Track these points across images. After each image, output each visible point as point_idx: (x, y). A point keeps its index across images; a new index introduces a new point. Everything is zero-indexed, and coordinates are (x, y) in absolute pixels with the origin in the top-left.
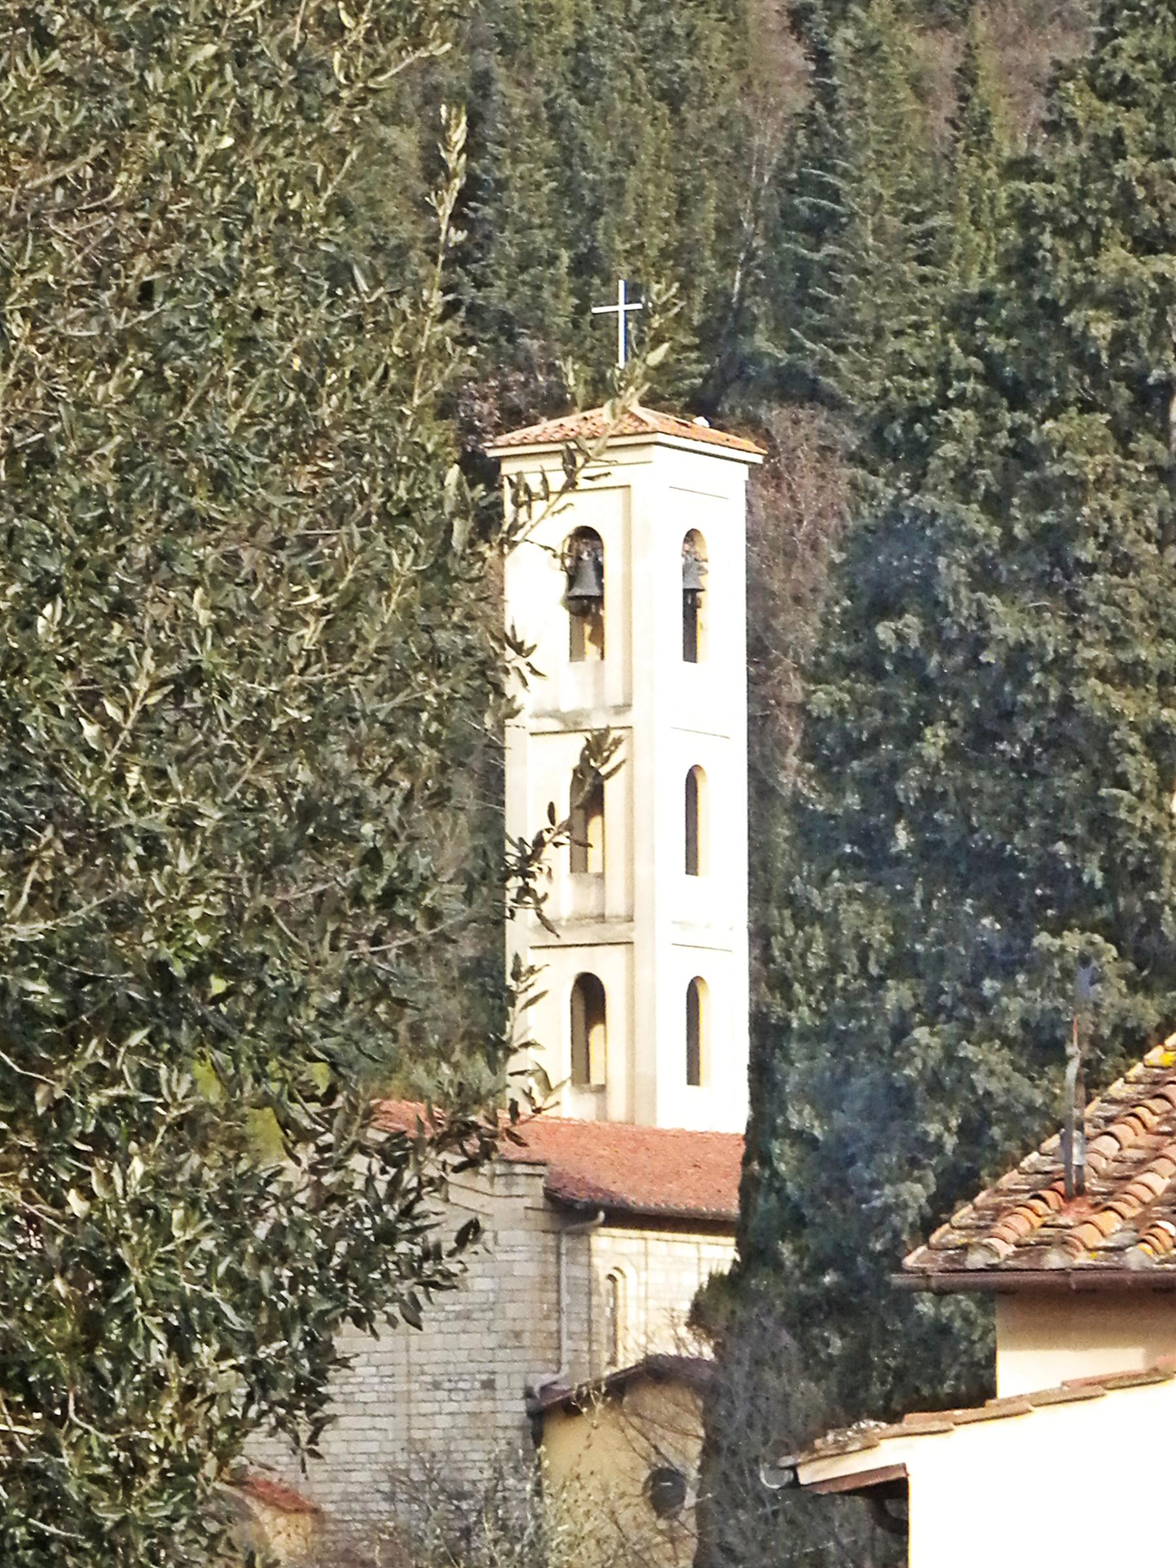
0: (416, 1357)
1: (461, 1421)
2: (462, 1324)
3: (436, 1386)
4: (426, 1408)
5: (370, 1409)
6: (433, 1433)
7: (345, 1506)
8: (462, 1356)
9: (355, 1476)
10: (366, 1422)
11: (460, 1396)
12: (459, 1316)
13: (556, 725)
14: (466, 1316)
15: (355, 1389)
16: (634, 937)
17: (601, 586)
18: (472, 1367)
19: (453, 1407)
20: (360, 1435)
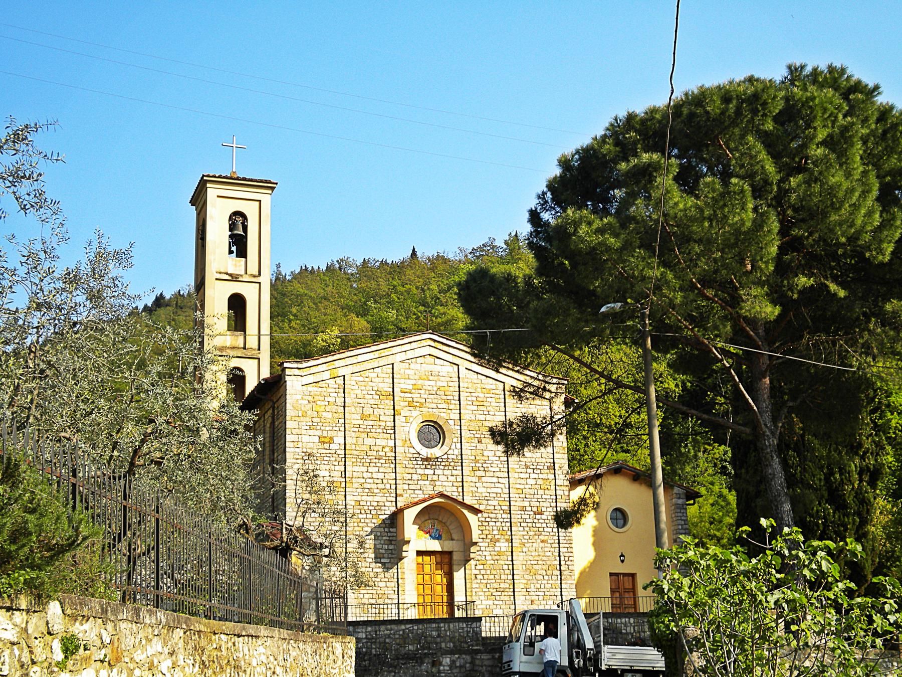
1: (539, 482)
3: (527, 467)
4: (522, 476)
5: (496, 474)
6: (527, 486)
10: (495, 480)
13: (230, 278)
16: (260, 356)
18: (544, 461)
19: (536, 476)
20: (493, 485)
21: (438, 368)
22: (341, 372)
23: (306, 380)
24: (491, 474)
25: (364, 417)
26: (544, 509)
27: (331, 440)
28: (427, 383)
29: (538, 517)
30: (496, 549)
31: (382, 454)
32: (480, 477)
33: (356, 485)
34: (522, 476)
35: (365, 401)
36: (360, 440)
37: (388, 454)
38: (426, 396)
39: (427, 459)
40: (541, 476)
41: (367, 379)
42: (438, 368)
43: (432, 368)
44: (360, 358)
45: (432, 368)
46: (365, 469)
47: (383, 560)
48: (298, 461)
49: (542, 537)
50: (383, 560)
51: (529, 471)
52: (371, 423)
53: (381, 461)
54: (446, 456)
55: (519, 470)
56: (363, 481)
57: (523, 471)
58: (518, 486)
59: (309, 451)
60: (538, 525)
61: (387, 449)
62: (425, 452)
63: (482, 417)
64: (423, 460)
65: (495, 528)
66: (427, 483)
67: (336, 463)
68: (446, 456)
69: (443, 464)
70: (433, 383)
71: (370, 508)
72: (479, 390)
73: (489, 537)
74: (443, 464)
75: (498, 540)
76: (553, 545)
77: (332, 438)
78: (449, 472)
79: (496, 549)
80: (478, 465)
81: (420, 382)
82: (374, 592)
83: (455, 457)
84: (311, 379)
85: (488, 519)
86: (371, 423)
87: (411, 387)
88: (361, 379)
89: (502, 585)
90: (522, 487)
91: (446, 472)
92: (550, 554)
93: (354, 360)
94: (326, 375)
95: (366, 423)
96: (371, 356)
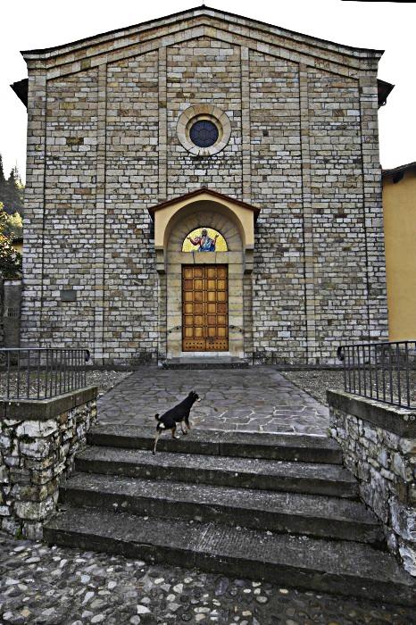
0: (314, 147)
1: (341, 179)
2: (340, 132)
3: (327, 161)
4: (319, 172)
6: (325, 185)
7: (272, 220)
8: (342, 147)
9: (277, 206)
10: (284, 179)
11: (342, 166)
12: (338, 128)
14: (344, 128)
15: (277, 162)
19: (338, 172)
20: (281, 185)
21: (215, 52)
22: (94, 63)
23: (50, 75)
25: (121, 113)
26: (346, 211)
27: (81, 141)
28: (200, 69)
29: (339, 220)
30: (284, 260)
31: (143, 154)
32: (265, 177)
34: (319, 172)
35: (123, 95)
36: (116, 140)
37: (151, 154)
38: (198, 85)
39: (198, 158)
40: (344, 172)
41: (125, 70)
42: (215, 52)
44: (116, 45)
46: (121, 172)
47: (140, 277)
48: (40, 166)
49: (344, 245)
50: (140, 277)
51: (328, 166)
52: (130, 119)
53: (141, 162)
54: (222, 154)
56: (119, 186)
57: (319, 166)
58: (314, 185)
59: (54, 154)
60: (339, 230)
61: (149, 149)
62: (196, 150)
63: (268, 106)
65: (283, 235)
67: (86, 167)
68: (222, 154)
69: (219, 162)
70: (208, 69)
71: (126, 217)
72: (266, 74)
73: (275, 246)
74: (219, 162)
75: (287, 250)
76: (360, 254)
78: (226, 172)
79: (284, 260)
80: (262, 162)
81: (191, 69)
82: (128, 313)
83: (233, 154)
84: (57, 73)
85: (274, 226)
86: (130, 119)
87: (179, 76)
88: (119, 70)
89: (290, 303)
90: (319, 185)
91: (221, 173)
92: (354, 264)
94: (76, 67)
96: (131, 41)
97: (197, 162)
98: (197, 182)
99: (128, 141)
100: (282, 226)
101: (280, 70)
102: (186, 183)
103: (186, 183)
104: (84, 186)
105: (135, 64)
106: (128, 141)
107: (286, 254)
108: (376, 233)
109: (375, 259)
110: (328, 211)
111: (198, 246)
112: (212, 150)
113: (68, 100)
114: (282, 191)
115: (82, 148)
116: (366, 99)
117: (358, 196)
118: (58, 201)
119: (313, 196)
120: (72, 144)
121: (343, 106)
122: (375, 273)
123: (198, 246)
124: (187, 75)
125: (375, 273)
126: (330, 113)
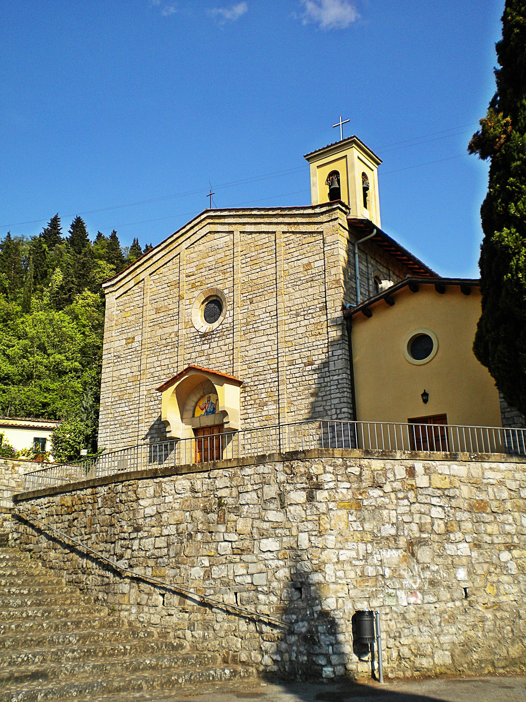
1: (311, 328)
3: (297, 315)
4: (292, 326)
6: (296, 337)
7: (256, 378)
10: (265, 338)
17: (339, 185)
22: (141, 277)
23: (118, 294)
24: (261, 333)
30: (264, 413)
31: (169, 340)
33: (149, 376)
34: (292, 326)
39: (204, 335)
43: (208, 245)
44: (155, 259)
45: (208, 245)
51: (299, 318)
54: (221, 327)
55: (289, 321)
57: (293, 320)
61: (173, 335)
64: (202, 336)
66: (203, 358)
68: (221, 327)
69: (218, 335)
70: (211, 259)
73: (258, 401)
75: (266, 404)
77: (134, 338)
79: (264, 413)
83: (228, 325)
88: (157, 277)
92: (321, 409)
93: (151, 262)
95: (158, 315)
97: (203, 339)
98: (204, 356)
99: (160, 332)
100: (262, 382)
101: (264, 241)
102: (196, 357)
103: (196, 357)
104: (134, 374)
105: (166, 269)
106: (160, 332)
107: (265, 409)
108: (339, 375)
109: (337, 401)
110: (299, 361)
111: (204, 410)
112: (215, 325)
113: (127, 310)
114: (263, 350)
115: (135, 345)
116: (329, 248)
117: (324, 342)
118: (119, 390)
119: (287, 349)
120: (129, 343)
121: (311, 260)
122: (338, 415)
123: (204, 410)
124: (199, 267)
125: (338, 415)
126: (302, 269)
